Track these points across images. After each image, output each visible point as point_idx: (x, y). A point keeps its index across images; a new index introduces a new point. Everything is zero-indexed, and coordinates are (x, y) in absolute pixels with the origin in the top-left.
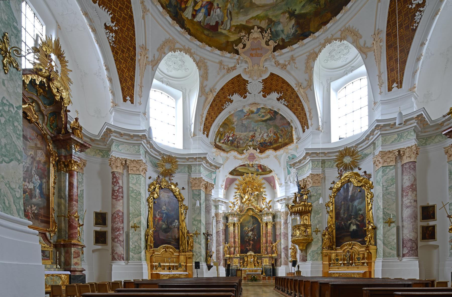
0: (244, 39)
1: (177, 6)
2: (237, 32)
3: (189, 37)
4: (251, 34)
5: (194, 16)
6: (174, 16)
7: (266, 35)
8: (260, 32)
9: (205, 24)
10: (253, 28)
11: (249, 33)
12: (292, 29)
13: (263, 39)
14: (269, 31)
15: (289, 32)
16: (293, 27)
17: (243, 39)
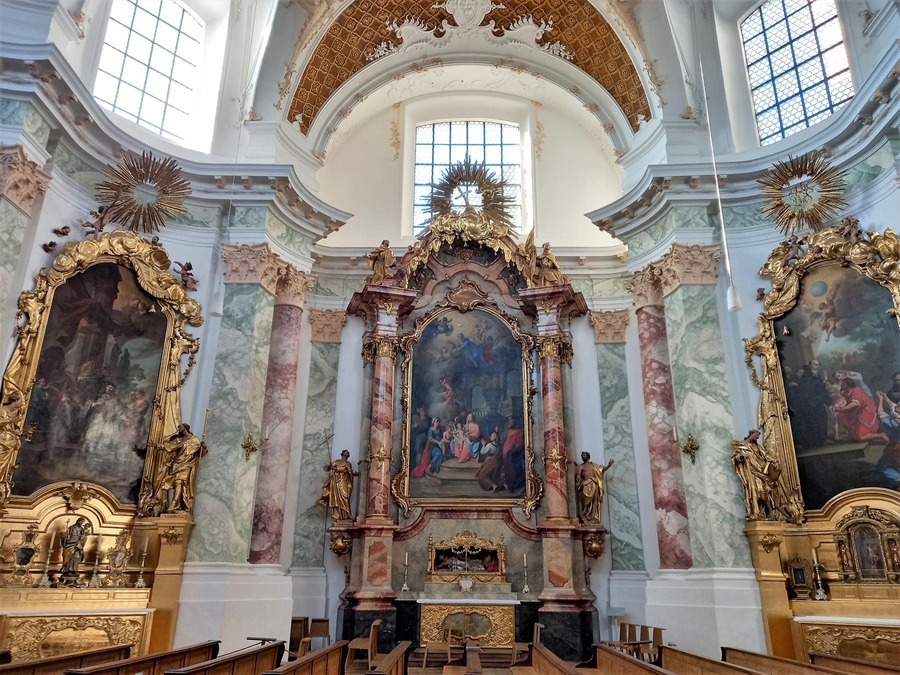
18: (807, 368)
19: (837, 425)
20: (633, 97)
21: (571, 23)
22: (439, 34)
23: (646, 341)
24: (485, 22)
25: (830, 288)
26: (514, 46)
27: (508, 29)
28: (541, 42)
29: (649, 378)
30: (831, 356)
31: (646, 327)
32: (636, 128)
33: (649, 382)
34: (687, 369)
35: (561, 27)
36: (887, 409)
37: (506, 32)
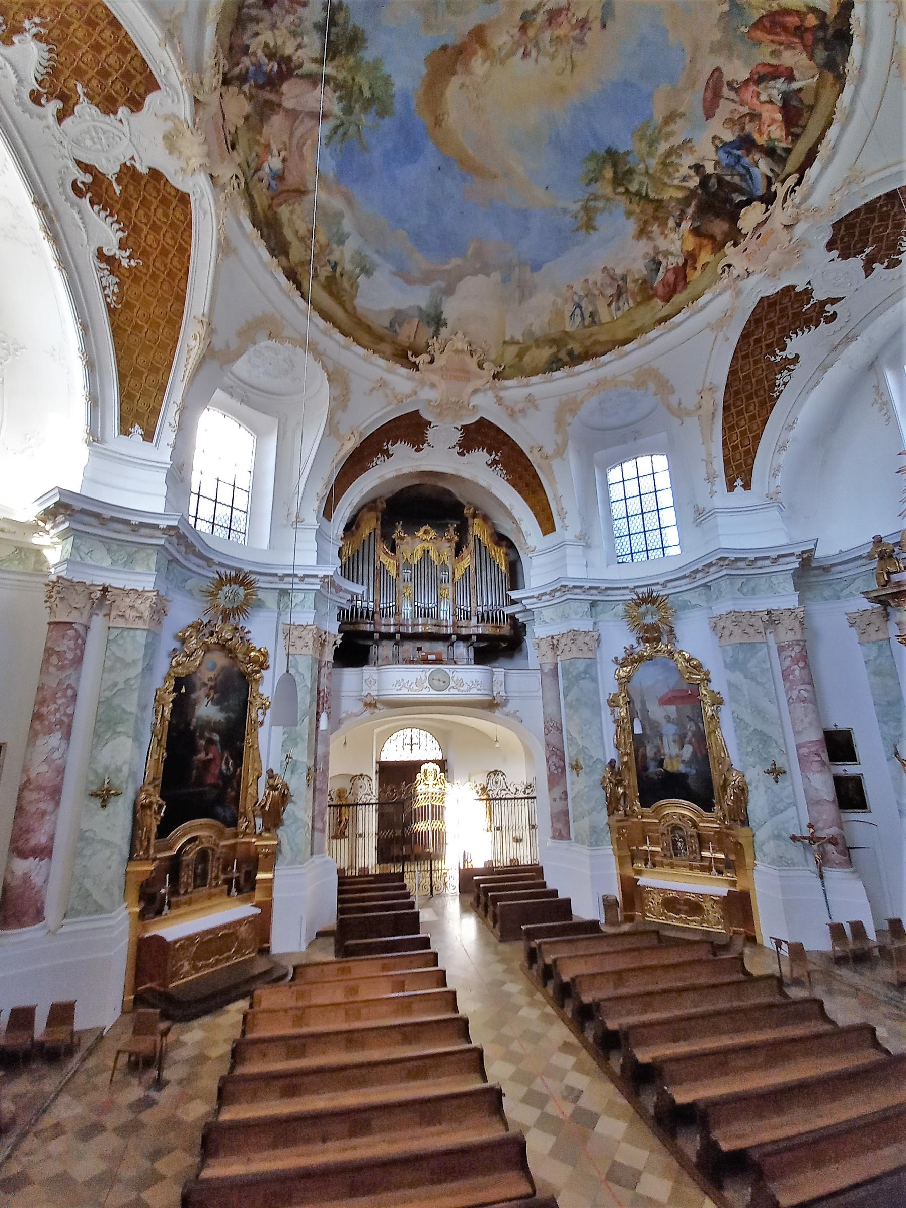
18: (188, 724)
19: (195, 771)
20: (141, 405)
21: (149, 288)
22: (36, 98)
23: (66, 662)
24: (86, 168)
25: (219, 667)
26: (74, 218)
27: (92, 203)
28: (100, 255)
29: (60, 706)
30: (206, 718)
31: (73, 646)
32: (125, 431)
33: (57, 710)
34: (124, 711)
35: (136, 279)
36: (227, 764)
37: (85, 202)
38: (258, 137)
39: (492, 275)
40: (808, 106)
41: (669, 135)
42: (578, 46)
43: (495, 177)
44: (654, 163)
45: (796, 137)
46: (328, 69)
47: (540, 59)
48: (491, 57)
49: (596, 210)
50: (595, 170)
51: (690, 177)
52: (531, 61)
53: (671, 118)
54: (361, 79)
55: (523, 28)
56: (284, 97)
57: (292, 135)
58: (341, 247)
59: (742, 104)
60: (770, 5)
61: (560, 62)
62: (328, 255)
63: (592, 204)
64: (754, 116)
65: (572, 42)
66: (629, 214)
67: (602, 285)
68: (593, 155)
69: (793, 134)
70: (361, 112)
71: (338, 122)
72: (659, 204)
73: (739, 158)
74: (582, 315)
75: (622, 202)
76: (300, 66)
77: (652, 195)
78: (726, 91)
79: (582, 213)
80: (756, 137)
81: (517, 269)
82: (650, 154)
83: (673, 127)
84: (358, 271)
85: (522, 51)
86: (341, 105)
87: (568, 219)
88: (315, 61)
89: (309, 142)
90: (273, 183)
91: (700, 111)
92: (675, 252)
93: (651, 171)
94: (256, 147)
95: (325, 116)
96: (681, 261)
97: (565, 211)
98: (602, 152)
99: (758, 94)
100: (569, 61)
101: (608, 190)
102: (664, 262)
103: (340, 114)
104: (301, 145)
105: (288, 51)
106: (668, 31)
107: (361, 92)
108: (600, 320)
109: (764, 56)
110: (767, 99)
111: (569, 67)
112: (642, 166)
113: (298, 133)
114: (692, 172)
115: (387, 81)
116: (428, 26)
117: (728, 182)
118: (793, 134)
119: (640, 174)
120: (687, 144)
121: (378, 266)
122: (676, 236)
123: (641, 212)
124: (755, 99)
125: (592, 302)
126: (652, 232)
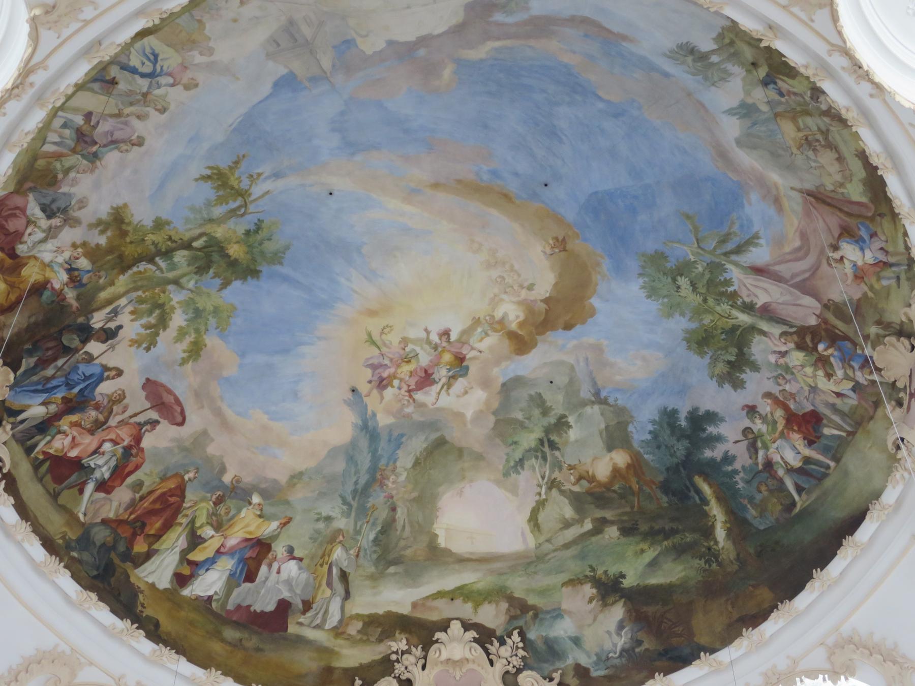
0: (406, 663)
1: (114, 547)
2: (373, 639)
3: (147, 646)
4: (436, 646)
5: (181, 580)
6: (95, 577)
7: (505, 651)
8: (475, 640)
9: (230, 607)
10: (444, 626)
11: (428, 643)
12: (619, 634)
13: (491, 663)
14: (516, 637)
15: (608, 645)
16: (621, 627)
17: (398, 661)
38: (870, 294)
39: (380, 45)
40: (59, 494)
41: (182, 333)
42: (375, 361)
43: (436, 186)
44: (176, 297)
45: (36, 466)
46: (743, 318)
47: (424, 335)
48: (499, 325)
49: (221, 200)
50: (261, 244)
51: (110, 320)
52: (435, 329)
53: (196, 351)
54: (695, 300)
55: (460, 359)
56: (818, 312)
57: (815, 269)
58: (750, 101)
59: (122, 423)
60: (187, 516)
61: (394, 339)
62: (780, 103)
63: (233, 205)
64: (98, 425)
65: (387, 362)
66: (159, 225)
67: (126, 123)
68: (277, 258)
69: (43, 462)
70: (695, 262)
71: (734, 257)
72: (123, 265)
73: (69, 386)
74: (134, 71)
75: (182, 229)
76: (784, 334)
77: (143, 266)
78: (154, 415)
79: (245, 184)
80: (74, 418)
81: (326, 63)
82: (188, 304)
83: (185, 344)
84: (714, 59)
85: (454, 337)
86: (727, 276)
87: (266, 169)
88: (764, 333)
89: (787, 249)
90: (863, 233)
91: (163, 379)
92: (43, 247)
93: (171, 287)
94: (877, 286)
95: (758, 271)
96: (21, 249)
97: (277, 175)
98: (264, 268)
99: (115, 443)
100: (379, 343)
101: (219, 232)
102: (44, 223)
103: (728, 266)
104: (801, 252)
105: (797, 358)
106: (271, 419)
107: (693, 285)
108: (92, 90)
109: (146, 474)
110: (101, 450)
111: (376, 337)
112: (191, 285)
113: (804, 265)
114: (112, 325)
115: (652, 292)
116: (598, 349)
117: (55, 359)
118: (43, 462)
119: (184, 275)
120: (149, 342)
121: (665, 55)
122: (60, 259)
123: (143, 240)
124: (113, 436)
125: (130, 93)
126: (102, 232)
